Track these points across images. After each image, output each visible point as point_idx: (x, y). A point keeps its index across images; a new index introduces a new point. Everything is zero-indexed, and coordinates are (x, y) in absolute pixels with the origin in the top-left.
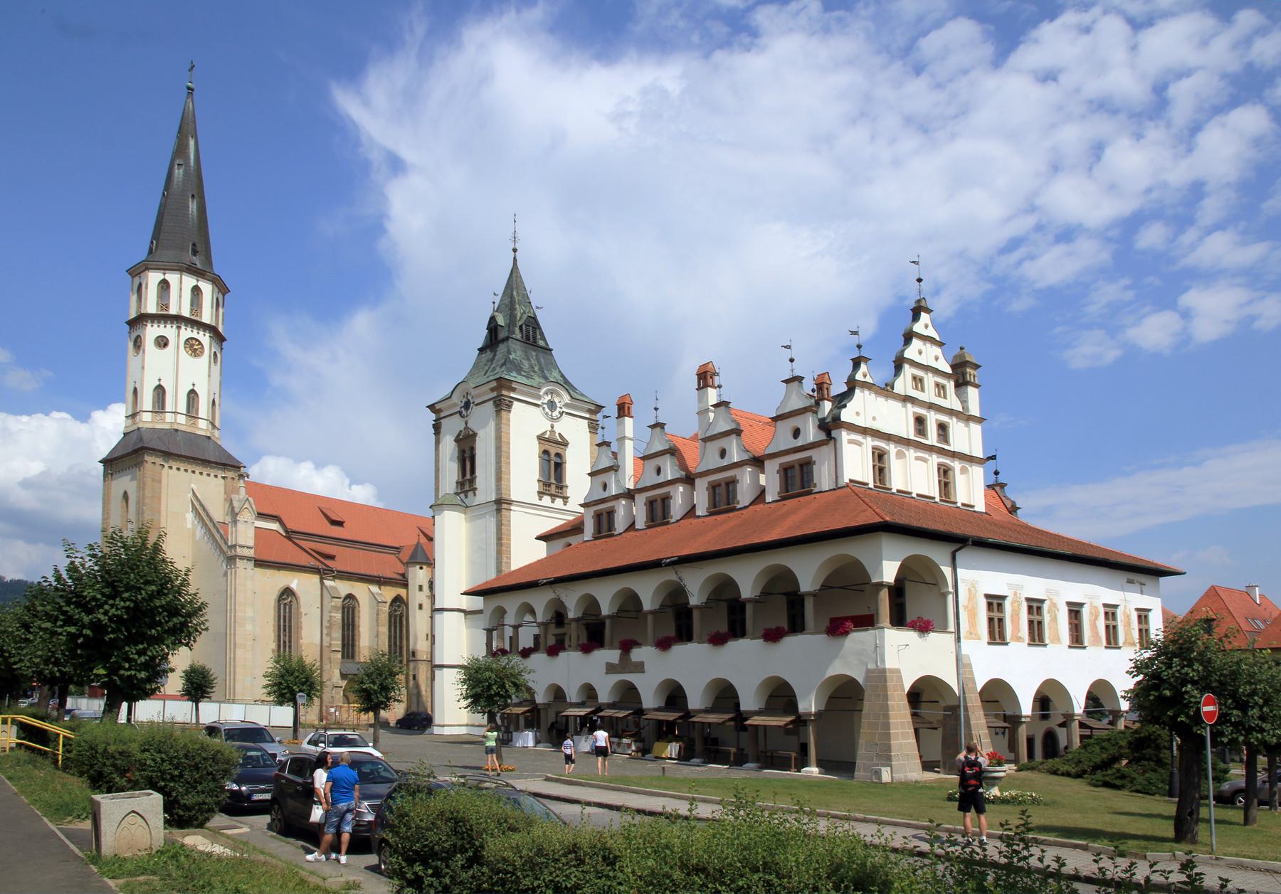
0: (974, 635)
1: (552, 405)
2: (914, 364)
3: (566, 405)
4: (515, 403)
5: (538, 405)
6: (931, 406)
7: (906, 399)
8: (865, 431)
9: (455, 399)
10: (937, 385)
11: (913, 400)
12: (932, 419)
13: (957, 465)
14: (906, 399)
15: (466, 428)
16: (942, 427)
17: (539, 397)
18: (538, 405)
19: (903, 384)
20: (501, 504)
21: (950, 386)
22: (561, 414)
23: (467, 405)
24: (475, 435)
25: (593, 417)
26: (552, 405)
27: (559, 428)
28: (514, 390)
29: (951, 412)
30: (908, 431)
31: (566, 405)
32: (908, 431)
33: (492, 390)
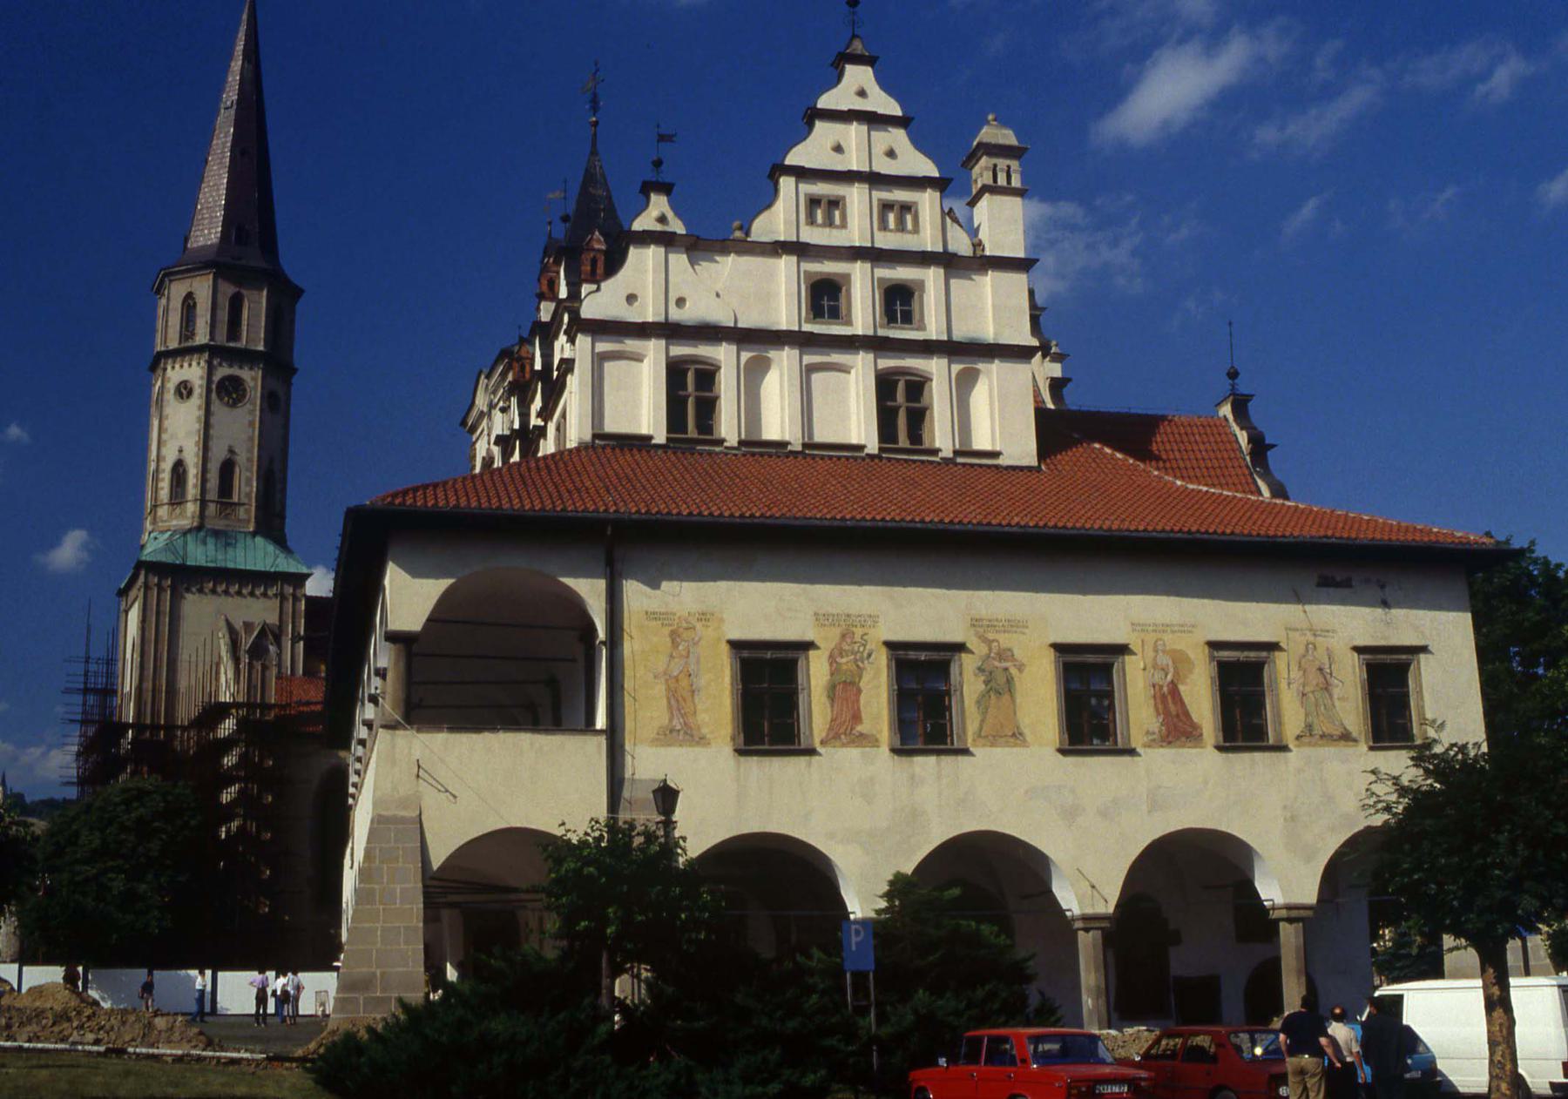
0: (682, 732)
2: (802, 173)
6: (856, 254)
7: (779, 248)
8: (643, 330)
10: (886, 207)
11: (800, 250)
12: (862, 286)
13: (937, 369)
14: (779, 248)
16: (898, 301)
19: (780, 218)
21: (928, 203)
29: (923, 259)
30: (785, 312)
32: (785, 312)
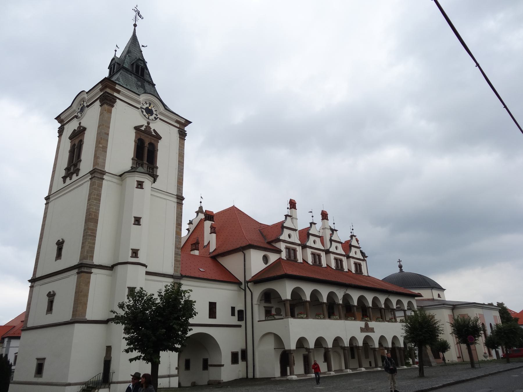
1: (149, 112)
3: (161, 113)
4: (117, 100)
5: (138, 108)
9: (74, 107)
15: (80, 127)
17: (139, 102)
18: (138, 108)
20: (97, 174)
22: (156, 119)
23: (82, 110)
24: (85, 129)
25: (181, 127)
26: (149, 112)
27: (153, 126)
28: (118, 92)
31: (161, 113)
33: (101, 90)
